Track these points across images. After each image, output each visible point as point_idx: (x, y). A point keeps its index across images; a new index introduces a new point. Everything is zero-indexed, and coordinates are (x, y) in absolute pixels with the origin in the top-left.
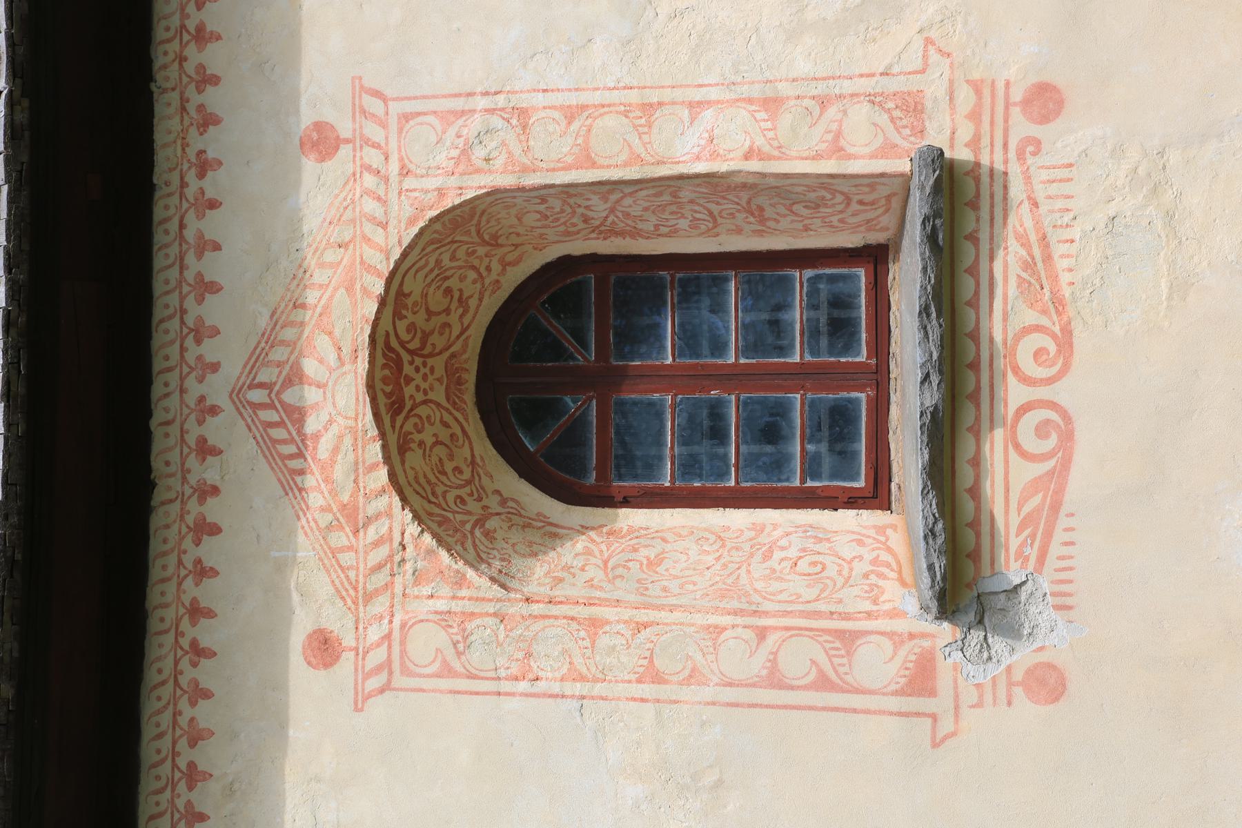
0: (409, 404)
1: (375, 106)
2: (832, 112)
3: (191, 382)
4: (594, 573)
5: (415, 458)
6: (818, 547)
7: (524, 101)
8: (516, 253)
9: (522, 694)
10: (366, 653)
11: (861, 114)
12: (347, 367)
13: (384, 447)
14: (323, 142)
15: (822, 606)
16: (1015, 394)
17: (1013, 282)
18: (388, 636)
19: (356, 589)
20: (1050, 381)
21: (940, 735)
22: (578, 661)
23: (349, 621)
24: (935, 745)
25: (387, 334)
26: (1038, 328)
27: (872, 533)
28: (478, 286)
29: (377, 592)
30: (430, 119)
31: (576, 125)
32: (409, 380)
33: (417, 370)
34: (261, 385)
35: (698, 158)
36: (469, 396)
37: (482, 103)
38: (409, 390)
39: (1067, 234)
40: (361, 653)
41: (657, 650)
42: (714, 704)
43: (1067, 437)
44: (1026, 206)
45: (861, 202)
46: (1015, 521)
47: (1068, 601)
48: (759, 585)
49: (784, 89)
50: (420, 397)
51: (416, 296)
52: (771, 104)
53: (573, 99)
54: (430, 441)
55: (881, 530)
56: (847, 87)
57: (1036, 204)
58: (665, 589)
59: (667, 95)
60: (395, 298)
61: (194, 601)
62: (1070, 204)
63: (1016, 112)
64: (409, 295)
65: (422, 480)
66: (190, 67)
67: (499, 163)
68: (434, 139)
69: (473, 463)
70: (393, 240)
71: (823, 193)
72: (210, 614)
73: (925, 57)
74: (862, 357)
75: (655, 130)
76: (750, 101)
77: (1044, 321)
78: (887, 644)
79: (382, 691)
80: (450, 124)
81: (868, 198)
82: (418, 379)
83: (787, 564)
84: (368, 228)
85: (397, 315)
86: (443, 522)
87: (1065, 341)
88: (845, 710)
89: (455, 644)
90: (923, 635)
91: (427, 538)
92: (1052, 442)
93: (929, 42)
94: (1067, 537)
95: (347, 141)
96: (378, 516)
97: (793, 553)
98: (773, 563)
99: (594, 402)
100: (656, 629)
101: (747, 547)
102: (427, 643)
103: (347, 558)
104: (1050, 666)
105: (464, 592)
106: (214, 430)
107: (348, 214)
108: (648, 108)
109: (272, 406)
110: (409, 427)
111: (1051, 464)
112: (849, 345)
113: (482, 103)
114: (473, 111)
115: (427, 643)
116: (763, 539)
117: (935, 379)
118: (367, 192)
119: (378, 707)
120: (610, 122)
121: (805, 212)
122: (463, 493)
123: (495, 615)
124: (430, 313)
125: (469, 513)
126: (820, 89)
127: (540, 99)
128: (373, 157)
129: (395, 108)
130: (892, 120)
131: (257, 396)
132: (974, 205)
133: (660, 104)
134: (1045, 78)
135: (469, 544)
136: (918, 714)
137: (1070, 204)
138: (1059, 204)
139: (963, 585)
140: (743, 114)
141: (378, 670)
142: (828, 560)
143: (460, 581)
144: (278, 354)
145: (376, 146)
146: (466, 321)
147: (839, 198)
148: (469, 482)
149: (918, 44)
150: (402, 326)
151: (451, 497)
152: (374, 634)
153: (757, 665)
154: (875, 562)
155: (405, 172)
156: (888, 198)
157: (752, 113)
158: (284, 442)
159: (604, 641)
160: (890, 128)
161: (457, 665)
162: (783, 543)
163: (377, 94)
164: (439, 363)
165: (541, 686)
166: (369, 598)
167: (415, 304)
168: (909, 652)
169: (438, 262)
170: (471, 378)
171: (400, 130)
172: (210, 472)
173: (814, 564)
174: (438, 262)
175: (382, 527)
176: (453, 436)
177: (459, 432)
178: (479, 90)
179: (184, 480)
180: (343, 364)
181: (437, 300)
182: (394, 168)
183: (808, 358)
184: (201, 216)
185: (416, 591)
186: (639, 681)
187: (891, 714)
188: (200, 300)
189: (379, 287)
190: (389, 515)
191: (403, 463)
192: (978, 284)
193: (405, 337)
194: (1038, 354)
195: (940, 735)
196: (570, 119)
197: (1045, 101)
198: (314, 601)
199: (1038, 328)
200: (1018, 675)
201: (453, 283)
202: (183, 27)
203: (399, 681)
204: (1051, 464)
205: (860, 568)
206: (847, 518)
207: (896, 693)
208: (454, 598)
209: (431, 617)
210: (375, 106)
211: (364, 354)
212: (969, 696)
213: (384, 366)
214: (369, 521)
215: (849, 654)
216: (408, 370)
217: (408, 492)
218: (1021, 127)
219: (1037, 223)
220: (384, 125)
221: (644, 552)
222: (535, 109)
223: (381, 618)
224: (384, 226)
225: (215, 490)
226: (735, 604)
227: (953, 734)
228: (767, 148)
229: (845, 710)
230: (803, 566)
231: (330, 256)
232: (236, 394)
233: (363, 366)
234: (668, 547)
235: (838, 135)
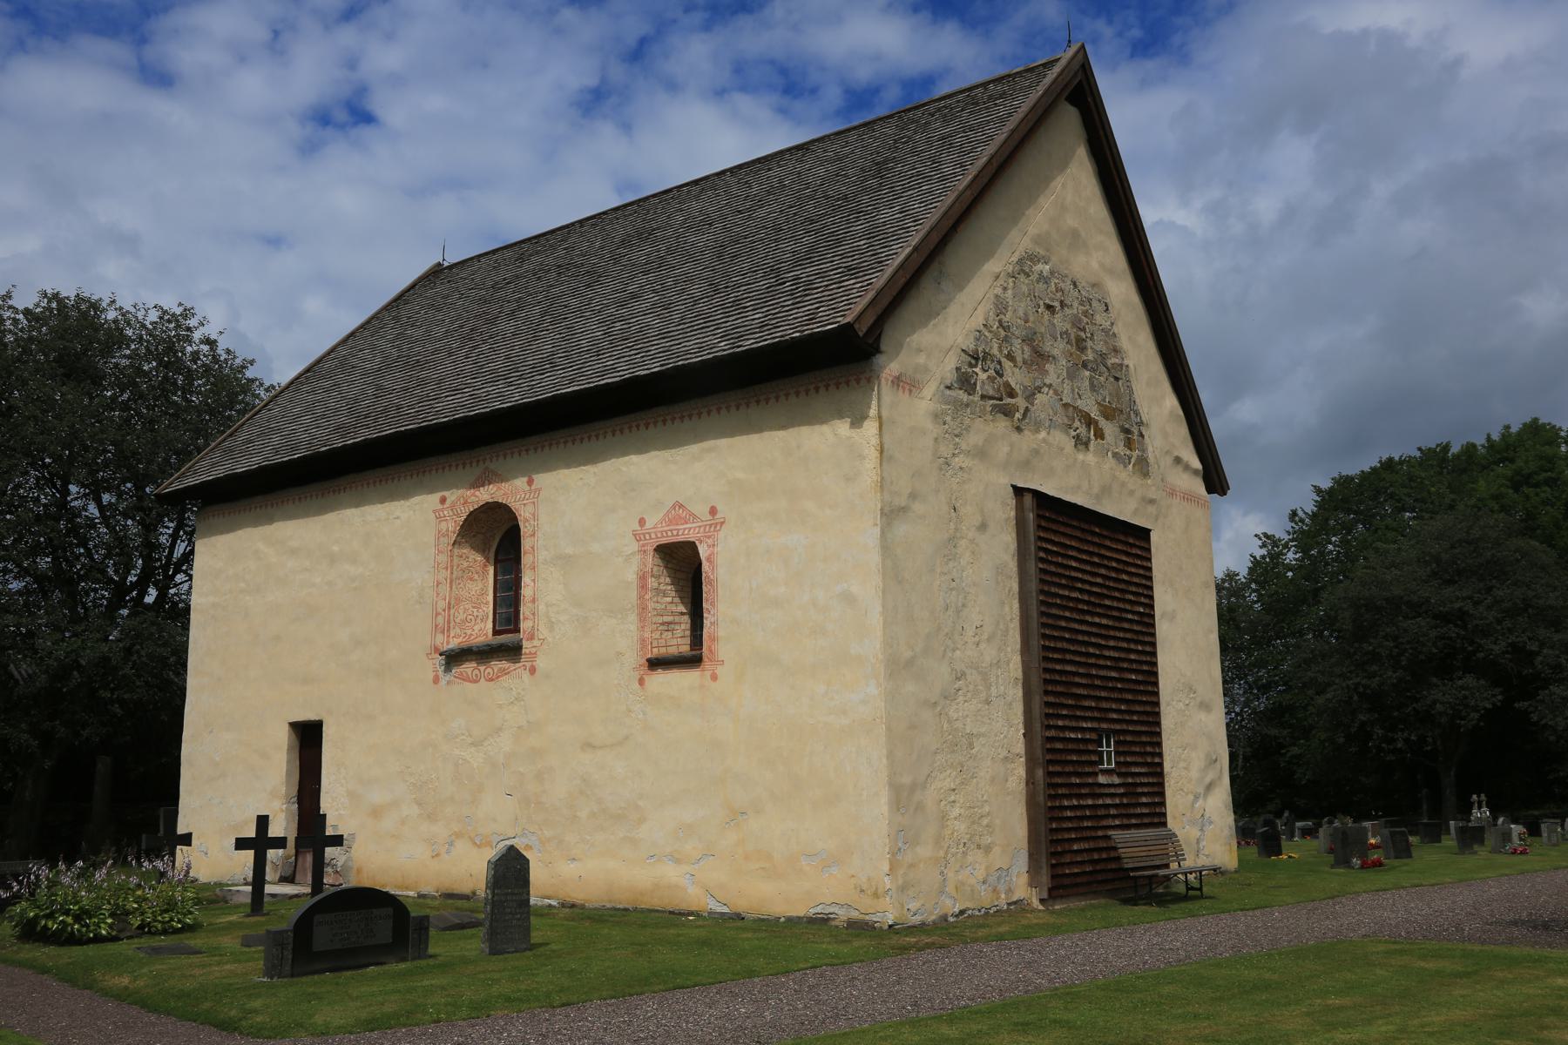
14: (530, 482)
16: (482, 668)
52: (533, 601)
115: (443, 526)
139: (454, 658)
197: (533, 671)
198: (452, 495)
206: (490, 625)
218: (528, 665)
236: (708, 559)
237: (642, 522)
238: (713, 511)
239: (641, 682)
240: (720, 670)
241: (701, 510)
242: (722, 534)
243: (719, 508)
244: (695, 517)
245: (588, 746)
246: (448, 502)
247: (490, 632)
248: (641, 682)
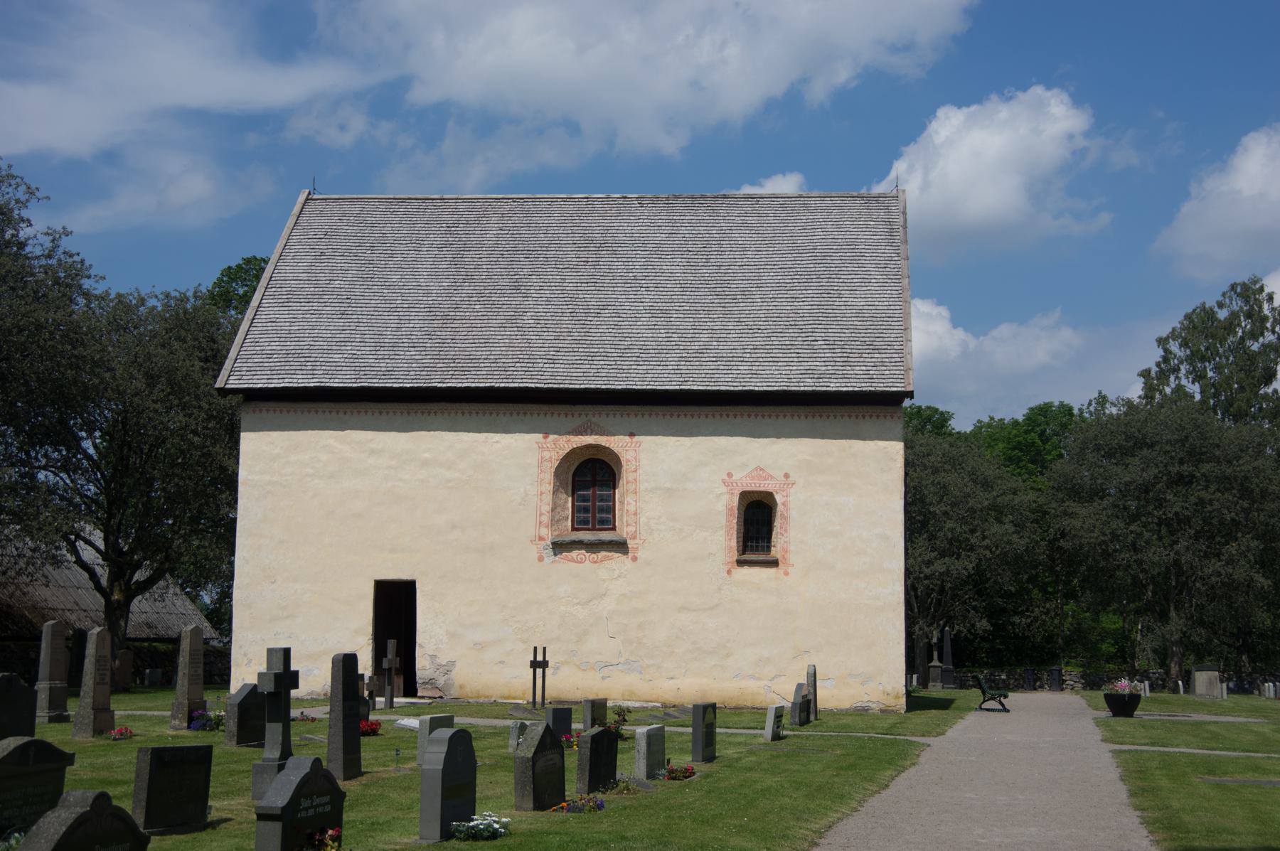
52: (636, 514)
60: (605, 448)
102: (547, 455)
115: (547, 455)
197: (635, 559)
236: (783, 504)
237: (730, 475)
238: (787, 476)
239: (729, 572)
240: (790, 570)
241: (779, 475)
242: (792, 491)
244: (772, 477)
245: (683, 609)
248: (729, 572)
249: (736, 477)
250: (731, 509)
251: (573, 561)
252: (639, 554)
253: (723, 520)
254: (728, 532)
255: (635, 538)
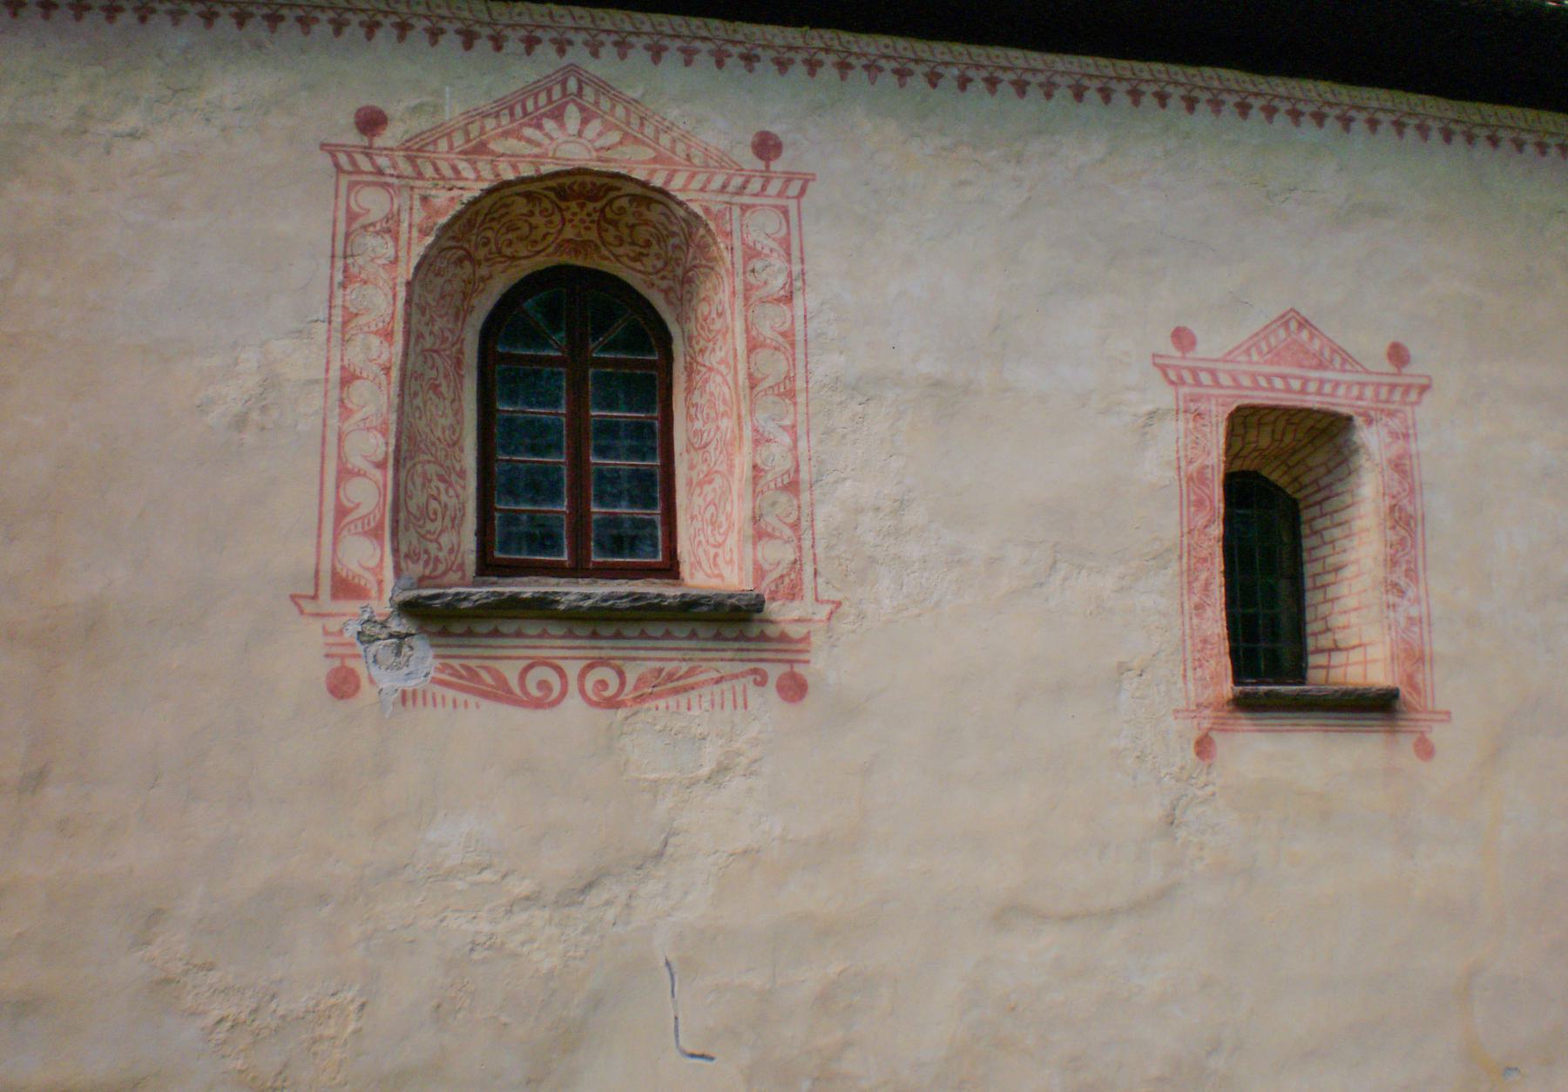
0: (563, 205)
1: (794, 189)
2: (788, 532)
3: (583, 36)
4: (429, 342)
5: (521, 206)
6: (448, 519)
7: (798, 301)
8: (675, 300)
9: (332, 278)
10: (367, 155)
11: (789, 554)
12: (594, 154)
13: (530, 180)
15: (402, 515)
17: (658, 665)
18: (380, 172)
19: (419, 150)
20: (582, 692)
21: (303, 603)
22: (362, 320)
23: (391, 143)
24: (293, 598)
25: (619, 189)
26: (623, 684)
27: (459, 560)
28: (650, 270)
29: (415, 166)
30: (784, 231)
31: (781, 339)
32: (582, 206)
33: (589, 215)
34: (580, 89)
35: (755, 430)
36: (565, 259)
37: (796, 268)
38: (573, 206)
39: (694, 703)
40: (368, 152)
41: (368, 383)
42: (325, 425)
43: (538, 704)
44: (715, 675)
45: (716, 555)
46: (473, 663)
47: (410, 703)
48: (419, 468)
49: (805, 497)
50: (568, 215)
51: (648, 215)
52: (792, 486)
53: (799, 337)
54: (533, 220)
55: (461, 567)
56: (807, 544)
57: (718, 681)
58: (416, 394)
59: (801, 409)
61: (412, 27)
62: (717, 707)
63: (785, 668)
64: (649, 209)
65: (503, 211)
66: (821, 56)
67: (751, 279)
68: (769, 231)
69: (513, 258)
70: (692, 195)
71: (725, 526)
72: (401, 38)
73: (828, 601)
74: (595, 558)
75: (777, 399)
76: (797, 471)
77: (629, 687)
78: (373, 563)
79: (337, 165)
80: (780, 244)
81: (720, 560)
82: (583, 215)
83: (434, 492)
84: (702, 178)
85: (634, 198)
86: (470, 224)
87: (612, 703)
88: (320, 528)
89: (373, 224)
90: (381, 591)
91: (459, 207)
92: (535, 692)
93: (839, 604)
94: (460, 702)
95: (768, 166)
96: (476, 170)
97: (444, 498)
98: (435, 483)
99: (558, 354)
100: (384, 383)
101: (448, 463)
103: (443, 145)
104: (357, 687)
105: (415, 233)
106: (546, 52)
107: (712, 163)
108: (791, 394)
109: (564, 94)
110: (546, 204)
111: (517, 690)
112: (602, 548)
113: (796, 268)
114: (789, 261)
115: (374, 203)
116: (454, 478)
117: (588, 603)
118: (730, 178)
119: (325, 161)
120: (783, 366)
121: (708, 516)
122: (493, 246)
123: (397, 258)
124: (632, 227)
125: (476, 248)
126: (804, 524)
127: (800, 313)
128: (755, 185)
129: (792, 204)
130: (782, 577)
131: (572, 85)
132: (718, 637)
133: (795, 404)
134: (810, 690)
135: (453, 243)
136: (317, 585)
137: (717, 707)
138: (717, 699)
140: (788, 464)
141: (353, 163)
142: (438, 523)
143: (424, 233)
144: (605, 104)
145: (764, 188)
146: (625, 259)
147: (720, 539)
148: (499, 252)
149: (837, 596)
150: (624, 202)
151: (489, 234)
152: (382, 161)
153: (356, 461)
154: (437, 559)
155: (744, 208)
156: (720, 576)
157: (788, 472)
158: (536, 103)
159: (375, 341)
160: (775, 575)
161: (356, 225)
162: (451, 492)
163: (803, 191)
164: (592, 235)
165: (339, 293)
166: (411, 160)
167: (641, 214)
168: (369, 581)
169: (673, 234)
170: (579, 262)
171: (776, 207)
172: (513, 45)
173: (435, 513)
174: (673, 234)
175: (468, 173)
176: (535, 242)
177: (540, 247)
178: (807, 267)
179: (508, 26)
180: (597, 150)
181: (643, 233)
182: (746, 200)
183: (595, 517)
184: (711, 53)
185: (416, 197)
186: (343, 368)
187: (318, 564)
188: (647, 48)
189: (658, 182)
190: (479, 178)
191: (518, 194)
192: (656, 638)
193: (616, 204)
194: (603, 684)
195: (303, 603)
196: (783, 334)
197: (794, 689)
199: (623, 684)
200: (350, 663)
201: (655, 248)
202: (850, 54)
203: (344, 181)
204: (517, 690)
205: (432, 547)
206: (469, 542)
207: (334, 569)
208: (410, 226)
209: (396, 207)
210: (794, 189)
211: (604, 167)
212: (333, 625)
213: (594, 184)
214: (473, 163)
215: (365, 533)
216: (590, 206)
217: (495, 196)
219: (704, 683)
220: (780, 194)
221: (444, 384)
222: (791, 309)
223: (395, 168)
224: (703, 190)
225: (498, 48)
226: (405, 447)
227: (302, 612)
228: (762, 482)
229: (320, 528)
230: (434, 504)
231: (680, 147)
232: (573, 69)
233: (596, 166)
234: (447, 403)
235: (771, 536)
237: (1182, 338)
238: (1398, 354)
241: (1370, 348)
242: (1425, 412)
243: (1414, 350)
244: (1347, 358)
246: (389, 137)
247: (471, 559)
249: (1211, 345)
250: (1200, 478)
251: (501, 693)
252: (819, 666)
253: (1168, 524)
254: (1191, 574)
255: (794, 593)
